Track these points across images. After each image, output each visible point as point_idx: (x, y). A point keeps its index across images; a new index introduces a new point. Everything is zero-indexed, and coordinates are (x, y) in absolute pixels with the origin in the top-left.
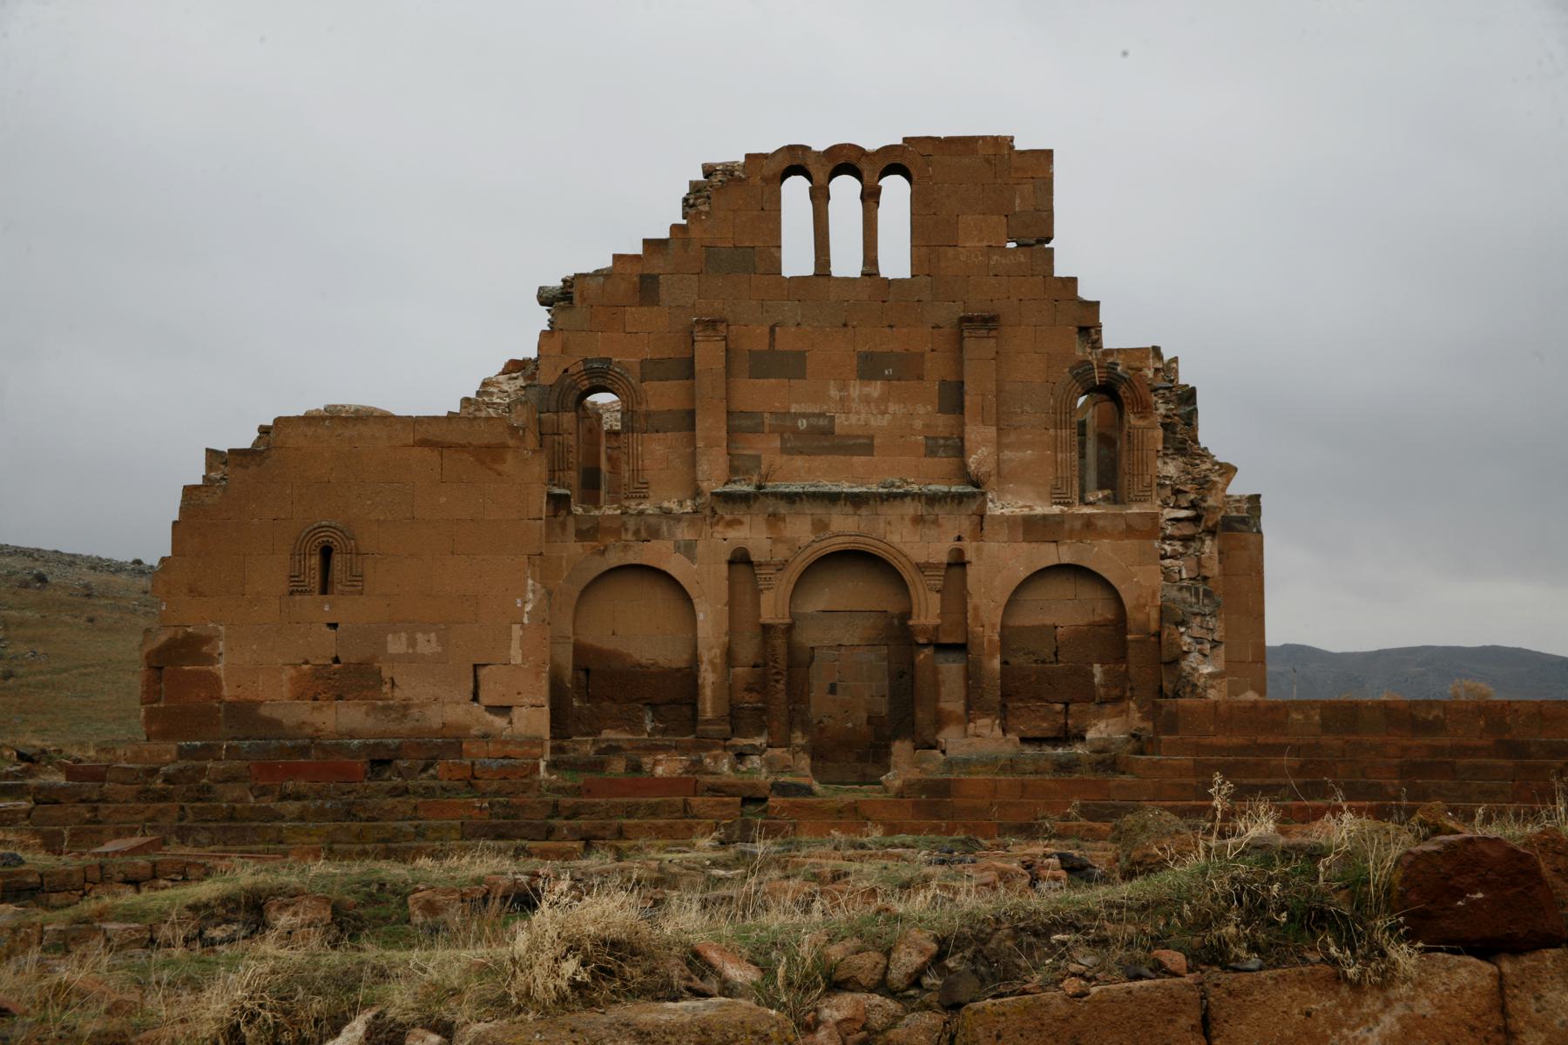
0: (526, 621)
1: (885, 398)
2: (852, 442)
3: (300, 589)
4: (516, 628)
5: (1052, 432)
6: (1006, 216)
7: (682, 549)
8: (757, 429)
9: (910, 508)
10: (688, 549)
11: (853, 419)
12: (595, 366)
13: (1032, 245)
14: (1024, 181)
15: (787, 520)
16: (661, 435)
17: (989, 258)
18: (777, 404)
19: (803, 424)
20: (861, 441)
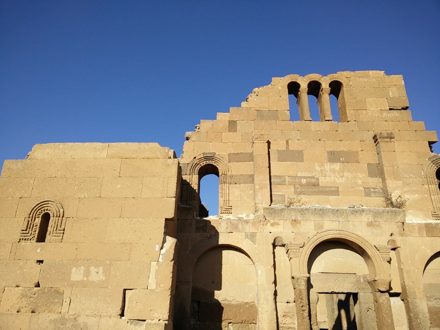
0: (160, 260)
1: (342, 170)
2: (329, 189)
3: (24, 238)
4: (154, 264)
5: (426, 186)
6: (387, 99)
7: (249, 236)
8: (283, 183)
9: (366, 218)
10: (252, 237)
11: (328, 179)
12: (208, 155)
13: (400, 110)
14: (392, 86)
15: (302, 223)
16: (237, 185)
17: (382, 114)
18: (291, 173)
19: (304, 181)
20: (333, 189)
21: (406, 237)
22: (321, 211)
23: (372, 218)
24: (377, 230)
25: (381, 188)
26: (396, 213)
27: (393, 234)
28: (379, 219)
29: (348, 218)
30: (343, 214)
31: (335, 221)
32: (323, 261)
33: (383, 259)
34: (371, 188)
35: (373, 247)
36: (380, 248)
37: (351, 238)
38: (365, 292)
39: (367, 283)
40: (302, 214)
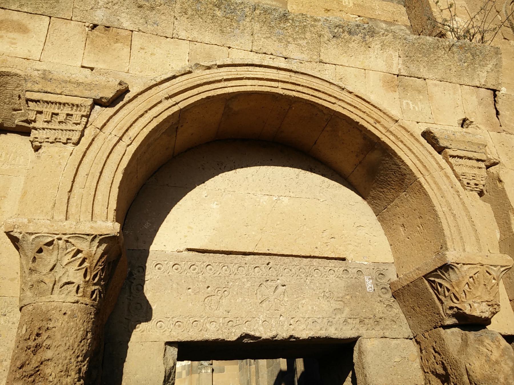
21: (509, 135)
22: (222, 6)
23: (401, 62)
24: (419, 103)
25: (406, 26)
26: (473, 56)
27: (467, 122)
28: (422, 70)
29: (322, 50)
30: (304, 33)
31: (272, 54)
32: (215, 206)
33: (465, 182)
34: (381, 21)
35: (417, 140)
36: (448, 138)
37: (333, 100)
38: (387, 334)
39: (390, 294)
40: (140, 7)
